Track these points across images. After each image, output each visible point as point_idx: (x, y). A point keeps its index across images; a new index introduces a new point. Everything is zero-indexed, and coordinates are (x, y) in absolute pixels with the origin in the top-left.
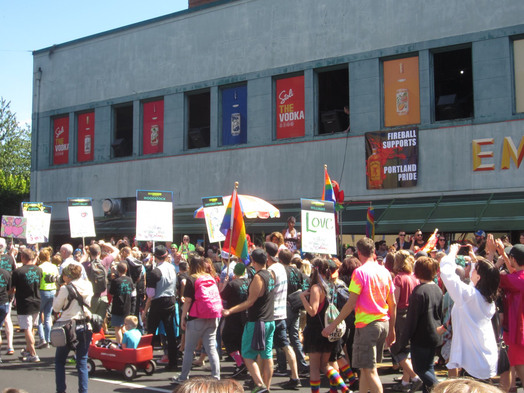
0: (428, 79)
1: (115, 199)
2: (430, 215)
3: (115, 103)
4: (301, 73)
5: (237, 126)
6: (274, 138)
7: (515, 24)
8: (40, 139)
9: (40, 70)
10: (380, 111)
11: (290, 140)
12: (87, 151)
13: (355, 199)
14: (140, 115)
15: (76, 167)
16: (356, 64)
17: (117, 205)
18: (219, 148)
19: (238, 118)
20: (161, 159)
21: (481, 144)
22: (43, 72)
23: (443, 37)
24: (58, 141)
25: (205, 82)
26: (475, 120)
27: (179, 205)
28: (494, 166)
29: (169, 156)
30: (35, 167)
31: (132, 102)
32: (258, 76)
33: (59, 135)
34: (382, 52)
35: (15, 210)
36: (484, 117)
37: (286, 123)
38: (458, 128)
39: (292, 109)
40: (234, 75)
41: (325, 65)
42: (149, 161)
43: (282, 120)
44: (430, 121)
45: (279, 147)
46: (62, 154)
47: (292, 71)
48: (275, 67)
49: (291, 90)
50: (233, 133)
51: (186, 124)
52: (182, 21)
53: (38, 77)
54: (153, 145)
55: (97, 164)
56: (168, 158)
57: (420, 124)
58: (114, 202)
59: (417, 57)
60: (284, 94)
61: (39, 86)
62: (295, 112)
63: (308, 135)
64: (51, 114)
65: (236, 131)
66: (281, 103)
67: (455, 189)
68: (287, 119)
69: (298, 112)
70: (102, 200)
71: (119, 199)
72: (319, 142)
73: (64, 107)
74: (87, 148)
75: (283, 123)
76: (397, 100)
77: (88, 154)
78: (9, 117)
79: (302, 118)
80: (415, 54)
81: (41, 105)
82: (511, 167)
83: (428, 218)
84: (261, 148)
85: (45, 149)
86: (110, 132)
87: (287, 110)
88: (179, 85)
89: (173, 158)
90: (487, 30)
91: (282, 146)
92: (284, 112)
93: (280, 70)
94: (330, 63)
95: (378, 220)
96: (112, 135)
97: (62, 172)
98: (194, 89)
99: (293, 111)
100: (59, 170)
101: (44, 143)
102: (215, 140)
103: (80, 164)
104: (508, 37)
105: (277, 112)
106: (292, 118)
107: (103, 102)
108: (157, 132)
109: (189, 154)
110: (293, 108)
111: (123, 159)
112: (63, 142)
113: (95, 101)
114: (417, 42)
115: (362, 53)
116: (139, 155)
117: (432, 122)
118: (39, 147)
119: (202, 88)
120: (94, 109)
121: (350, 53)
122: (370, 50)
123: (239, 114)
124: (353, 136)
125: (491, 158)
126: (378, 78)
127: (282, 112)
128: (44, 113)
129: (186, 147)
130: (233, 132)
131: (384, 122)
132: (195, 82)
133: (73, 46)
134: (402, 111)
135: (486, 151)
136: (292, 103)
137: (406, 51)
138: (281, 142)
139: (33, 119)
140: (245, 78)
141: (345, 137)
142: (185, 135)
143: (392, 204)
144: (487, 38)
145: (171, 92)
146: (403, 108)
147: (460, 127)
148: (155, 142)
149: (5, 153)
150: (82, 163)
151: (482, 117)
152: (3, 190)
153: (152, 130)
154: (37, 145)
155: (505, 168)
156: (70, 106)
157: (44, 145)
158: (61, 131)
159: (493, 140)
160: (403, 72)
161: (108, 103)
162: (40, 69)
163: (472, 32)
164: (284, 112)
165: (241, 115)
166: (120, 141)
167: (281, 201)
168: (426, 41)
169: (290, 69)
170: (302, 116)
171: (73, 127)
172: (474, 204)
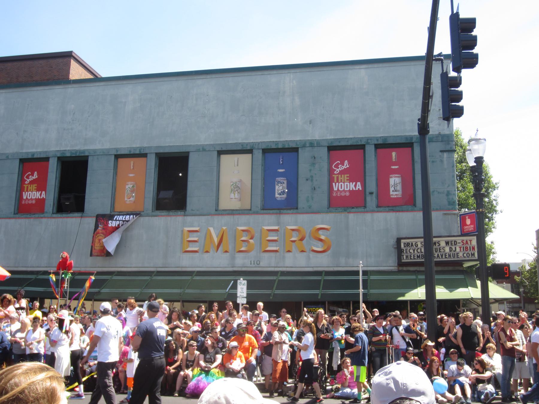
0: (153, 176)
2: (144, 286)
4: (362, 147)
5: (282, 190)
6: (262, 208)
7: (223, 143)
10: (112, 198)
15: (174, 216)
18: (262, 211)
19: (284, 183)
26: (367, 209)
28: (199, 249)
32: (312, 144)
34: (118, 150)
36: (194, 210)
37: (341, 192)
38: (173, 218)
39: (347, 180)
41: (68, 155)
43: (335, 189)
47: (38, 157)
48: (24, 151)
49: (346, 161)
50: (277, 197)
54: (128, 202)
60: (338, 164)
62: (351, 183)
65: (281, 195)
66: (335, 173)
67: (167, 266)
68: (341, 188)
69: (354, 183)
72: (56, 220)
74: (396, 191)
75: (337, 192)
76: (126, 191)
79: (359, 189)
80: (250, 151)
82: (211, 251)
83: (185, 288)
84: (3, 220)
87: (341, 180)
90: (202, 144)
91: (22, 219)
94: (73, 154)
99: (349, 181)
100: (282, 216)
104: (373, 146)
105: (331, 181)
106: (347, 188)
110: (348, 178)
111: (71, 215)
112: (35, 189)
119: (65, 155)
125: (197, 243)
126: (112, 171)
127: (335, 181)
129: (55, 211)
130: (277, 195)
131: (218, 206)
135: (194, 237)
137: (239, 148)
138: (22, 216)
142: (55, 198)
143: (195, 276)
144: (316, 145)
146: (130, 197)
147: (175, 217)
151: (192, 210)
155: (207, 252)
158: (33, 176)
159: (199, 229)
160: (133, 168)
164: (338, 181)
165: (287, 179)
169: (38, 154)
170: (359, 186)
171: (17, 174)
172: (273, 279)
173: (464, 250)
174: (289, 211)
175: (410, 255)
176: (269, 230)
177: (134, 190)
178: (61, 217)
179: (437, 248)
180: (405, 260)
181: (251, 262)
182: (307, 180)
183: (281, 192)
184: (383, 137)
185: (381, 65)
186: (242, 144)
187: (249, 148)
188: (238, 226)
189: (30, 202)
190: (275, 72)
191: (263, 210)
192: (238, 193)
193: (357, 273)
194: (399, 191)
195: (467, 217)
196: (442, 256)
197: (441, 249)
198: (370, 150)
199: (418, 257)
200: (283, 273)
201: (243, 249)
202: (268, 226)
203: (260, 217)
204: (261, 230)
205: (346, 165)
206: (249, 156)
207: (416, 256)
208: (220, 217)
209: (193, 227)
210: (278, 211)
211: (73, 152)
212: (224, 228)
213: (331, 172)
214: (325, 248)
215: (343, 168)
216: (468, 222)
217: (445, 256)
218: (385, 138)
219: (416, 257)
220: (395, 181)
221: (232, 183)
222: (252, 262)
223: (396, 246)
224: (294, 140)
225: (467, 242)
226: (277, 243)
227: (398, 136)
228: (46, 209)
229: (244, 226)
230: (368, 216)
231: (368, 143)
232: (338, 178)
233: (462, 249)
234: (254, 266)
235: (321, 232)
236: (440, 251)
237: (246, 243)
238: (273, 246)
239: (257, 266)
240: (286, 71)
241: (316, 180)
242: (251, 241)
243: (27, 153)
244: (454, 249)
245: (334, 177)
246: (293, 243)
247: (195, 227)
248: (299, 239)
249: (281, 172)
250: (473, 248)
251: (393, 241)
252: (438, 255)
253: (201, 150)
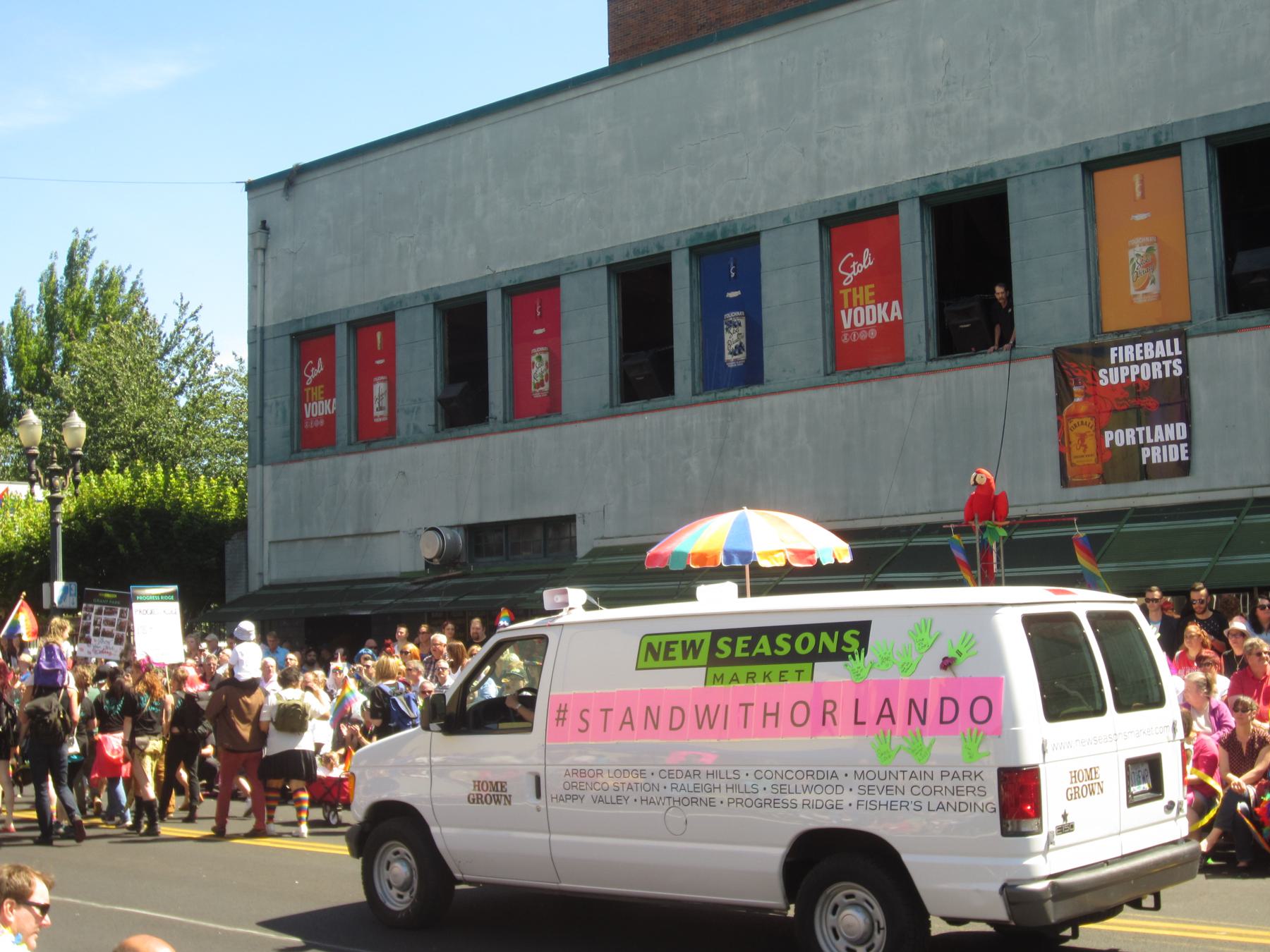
0: (1207, 211)
1: (451, 527)
3: (444, 297)
4: (891, 209)
5: (738, 343)
6: (829, 371)
8: (269, 388)
9: (264, 226)
10: (1090, 294)
11: (868, 373)
12: (380, 414)
13: (1033, 511)
14: (503, 325)
15: (355, 453)
16: (1026, 181)
17: (454, 543)
19: (740, 324)
20: (558, 427)
22: (272, 231)
23: (1240, 106)
24: (310, 391)
25: (658, 241)
27: (603, 538)
29: (575, 422)
30: (259, 457)
31: (484, 293)
32: (787, 221)
33: (313, 380)
35: (214, 559)
37: (859, 331)
40: (726, 220)
41: (948, 186)
42: (527, 434)
43: (847, 325)
44: (1215, 314)
45: (843, 391)
46: (322, 422)
47: (868, 205)
48: (828, 196)
49: (867, 250)
50: (729, 361)
51: (614, 342)
52: (599, 96)
53: (260, 244)
54: (537, 396)
55: (403, 444)
56: (573, 426)
58: (448, 536)
59: (1012, 190)
60: (850, 261)
61: (264, 265)
63: (912, 359)
64: (294, 330)
65: (735, 355)
66: (845, 284)
68: (859, 321)
69: (886, 304)
70: (419, 532)
71: (458, 526)
72: (941, 376)
73: (322, 311)
74: (381, 408)
75: (850, 333)
76: (1131, 266)
77: (382, 423)
78: (197, 339)
79: (896, 317)
81: (269, 309)
84: (800, 394)
85: (280, 414)
86: (433, 366)
87: (858, 300)
88: (596, 248)
89: (584, 425)
91: (849, 387)
92: (851, 306)
93: (839, 204)
94: (962, 183)
95: (876, 573)
96: (438, 375)
97: (323, 466)
98: (632, 256)
99: (873, 301)
100: (314, 462)
101: (279, 399)
102: (685, 378)
103: (363, 447)
105: (833, 305)
106: (871, 319)
107: (416, 295)
108: (547, 363)
109: (624, 415)
110: (873, 294)
111: (466, 431)
112: (322, 395)
113: (397, 294)
114: (1173, 120)
115: (1036, 155)
116: (505, 421)
117: (1222, 315)
118: (267, 410)
119: (650, 254)
120: (393, 313)
121: (1010, 156)
122: (1058, 147)
123: (742, 313)
124: (1024, 359)
126: (1082, 213)
127: (846, 304)
128: (278, 325)
129: (617, 398)
130: (728, 357)
131: (1100, 322)
132: (634, 240)
133: (338, 167)
134: (1144, 292)
136: (870, 283)
137: (1149, 144)
138: (847, 377)
139: (251, 343)
140: (755, 227)
141: (1005, 361)
145: (576, 267)
148: (541, 389)
149: (188, 425)
150: (368, 443)
152: (184, 513)
153: (534, 359)
154: (263, 405)
156: (336, 308)
157: (277, 404)
160: (1143, 196)
161: (427, 298)
162: (264, 222)
164: (851, 306)
165: (746, 316)
166: (457, 389)
167: (851, 522)
168: (1197, 119)
169: (864, 199)
170: (896, 313)
171: (345, 358)
177: (1154, 261)
178: (949, 369)
189: (317, 424)
205: (867, 260)
211: (960, 175)
218: (853, 200)
228: (909, 352)
232: (850, 295)
243: (836, 200)
245: (842, 295)
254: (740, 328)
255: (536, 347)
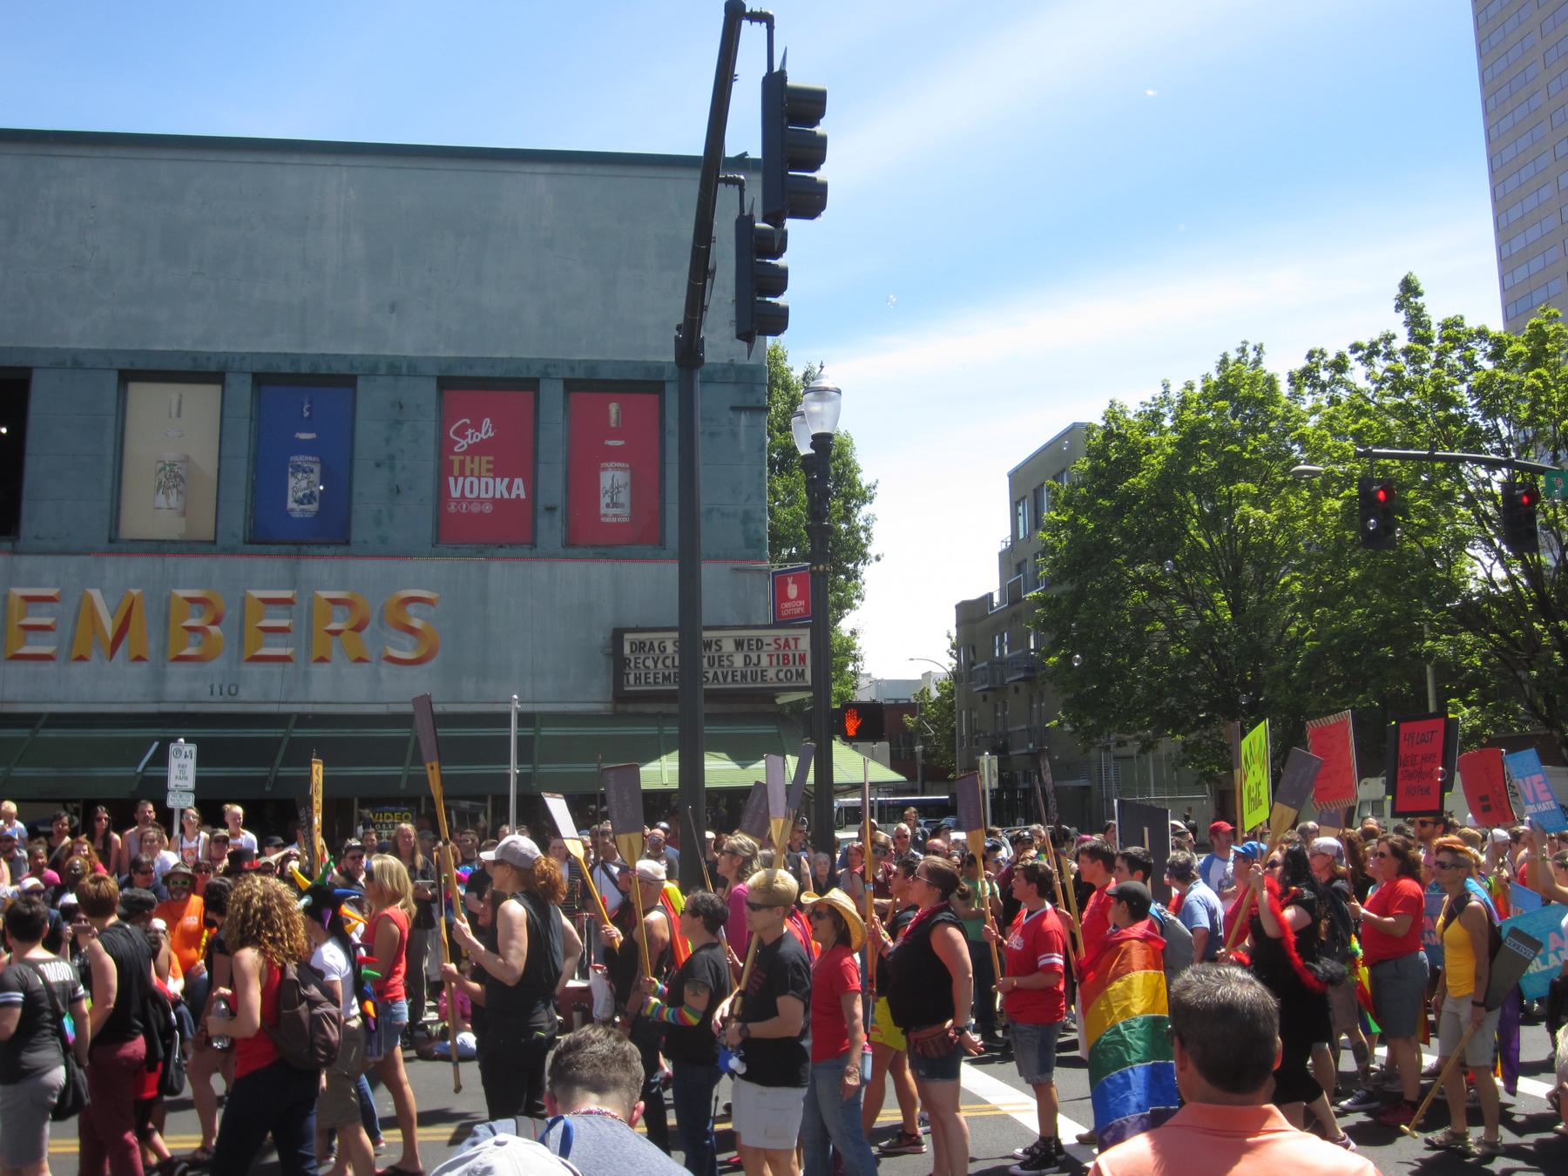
5: (307, 492)
6: (247, 539)
7: (136, 347)
18: (249, 546)
19: (312, 471)
21: (29, 599)
32: (397, 369)
37: (470, 503)
39: (488, 470)
43: (456, 494)
49: (488, 420)
50: (293, 510)
57: (214, 542)
60: (464, 427)
65: (302, 504)
68: (471, 492)
69: (506, 480)
74: (615, 505)
75: (459, 503)
79: (518, 496)
80: (214, 376)
87: (472, 471)
90: (71, 346)
92: (462, 474)
99: (492, 475)
100: (304, 562)
106: (487, 493)
110: (491, 466)
113: (525, 356)
125: (51, 633)
127: (456, 471)
130: (291, 505)
131: (117, 529)
135: (40, 615)
137: (186, 366)
144: (404, 371)
151: (37, 538)
155: (81, 658)
163: (36, 345)
164: (462, 474)
165: (322, 462)
170: (519, 489)
172: (273, 735)
173: (778, 663)
174: (324, 550)
175: (646, 674)
176: (266, 601)
179: (714, 657)
180: (631, 686)
181: (212, 687)
182: (378, 465)
183: (304, 495)
184: (585, 361)
185: (589, 169)
186: (194, 356)
187: (213, 367)
188: (175, 588)
190: (296, 159)
191: (251, 542)
192: (179, 492)
193: (503, 719)
194: (622, 506)
195: (790, 580)
196: (725, 678)
197: (725, 658)
198: (552, 393)
199: (666, 678)
200: (303, 720)
201: (189, 651)
202: (264, 587)
203: (242, 564)
204: (243, 600)
205: (487, 430)
206: (211, 392)
207: (661, 676)
208: (123, 560)
209: (38, 585)
210: (293, 548)
212: (135, 592)
213: (444, 446)
214: (423, 651)
215: (477, 437)
216: (793, 591)
217: (733, 676)
218: (593, 365)
219: (660, 680)
220: (613, 479)
221: (161, 465)
222: (217, 690)
223: (610, 650)
224: (345, 356)
225: (787, 644)
226: (289, 636)
227: (627, 362)
229: (194, 588)
230: (541, 570)
231: (548, 376)
232: (462, 463)
233: (775, 659)
234: (221, 698)
235: (411, 609)
236: (720, 665)
237: (199, 636)
238: (276, 645)
239: (230, 698)
240: (330, 160)
241: (404, 468)
242: (214, 630)
244: (755, 660)
245: (452, 461)
246: (335, 637)
247: (44, 586)
248: (353, 626)
249: (305, 440)
250: (802, 658)
251: (602, 637)
252: (716, 673)
253: (69, 364)
254: (312, 475)
255: (609, 460)
